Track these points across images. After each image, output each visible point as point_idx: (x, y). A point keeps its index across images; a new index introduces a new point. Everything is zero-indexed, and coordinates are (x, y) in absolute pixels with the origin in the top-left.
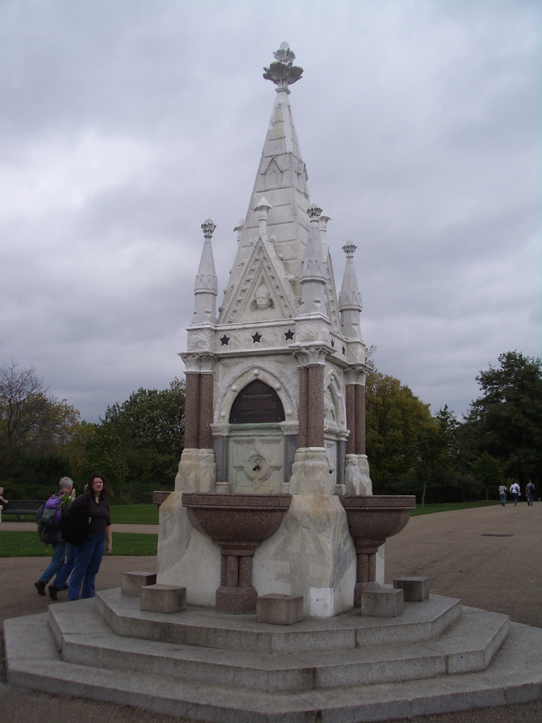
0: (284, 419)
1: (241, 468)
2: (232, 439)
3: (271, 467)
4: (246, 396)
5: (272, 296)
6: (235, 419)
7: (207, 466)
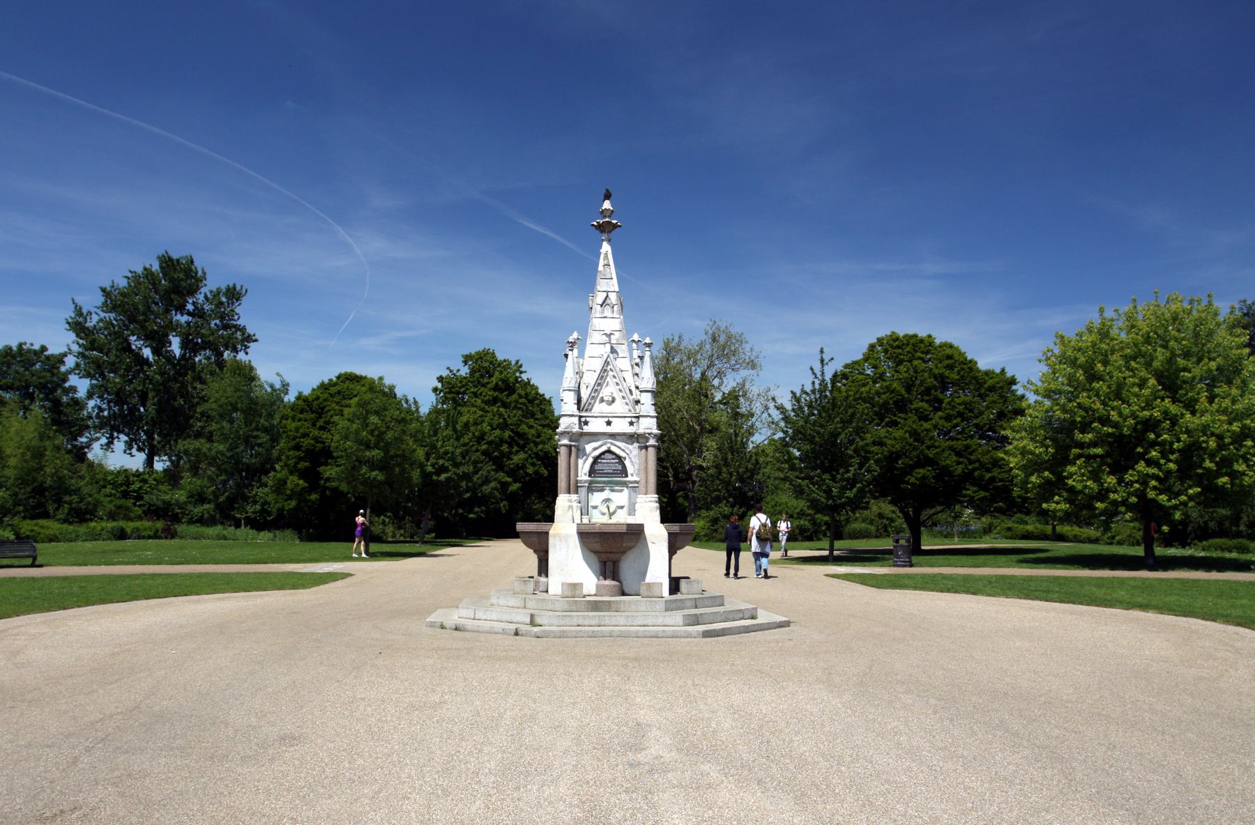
1: (595, 507)
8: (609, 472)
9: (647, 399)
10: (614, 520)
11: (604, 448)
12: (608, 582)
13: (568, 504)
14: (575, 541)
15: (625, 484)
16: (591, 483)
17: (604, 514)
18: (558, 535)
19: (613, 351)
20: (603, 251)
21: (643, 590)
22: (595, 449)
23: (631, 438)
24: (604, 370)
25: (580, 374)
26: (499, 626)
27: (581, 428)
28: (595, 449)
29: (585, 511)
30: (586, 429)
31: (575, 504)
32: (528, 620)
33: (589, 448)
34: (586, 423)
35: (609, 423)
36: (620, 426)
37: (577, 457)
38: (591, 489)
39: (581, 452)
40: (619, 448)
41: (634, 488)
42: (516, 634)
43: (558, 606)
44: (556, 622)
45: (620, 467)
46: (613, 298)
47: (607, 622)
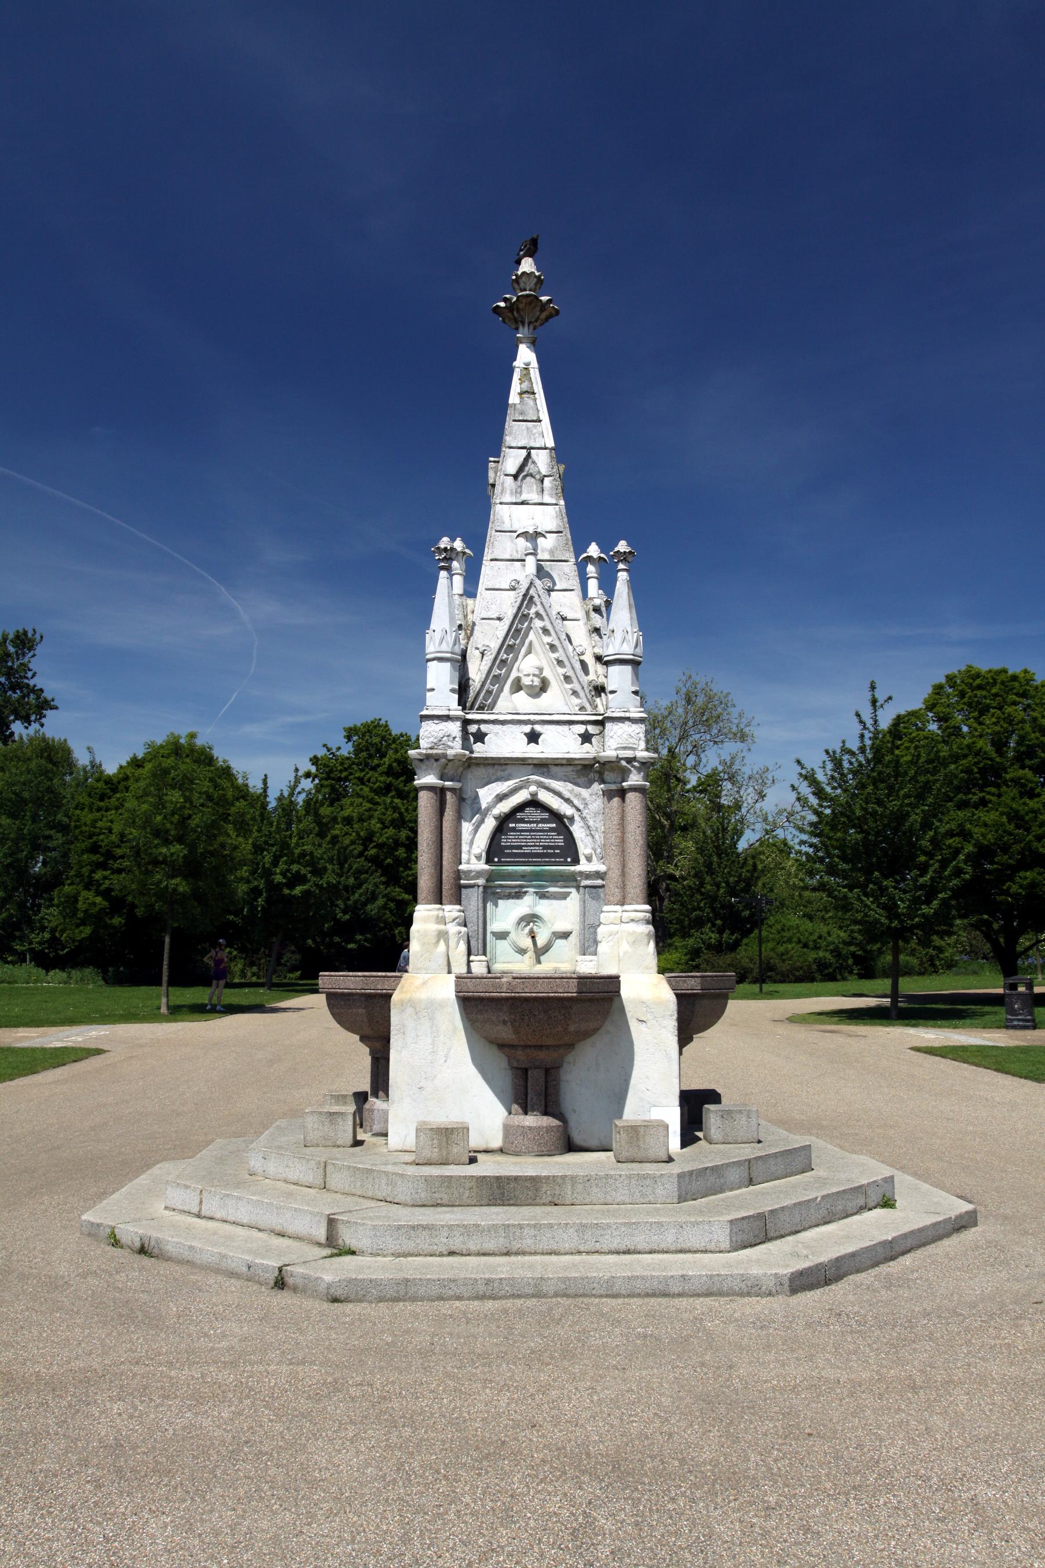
0: (576, 861)
1: (502, 936)
2: (489, 891)
5: (547, 673)
6: (496, 860)
8: (534, 851)
9: (620, 678)
10: (548, 966)
11: (522, 796)
12: (532, 1120)
13: (434, 927)
14: (452, 1019)
15: (572, 880)
16: (491, 877)
17: (522, 951)
18: (412, 1003)
19: (541, 572)
20: (518, 363)
21: (619, 1141)
22: (501, 798)
24: (521, 616)
25: (466, 629)
26: (238, 1257)
27: (466, 745)
28: (501, 798)
29: (477, 943)
30: (480, 750)
31: (453, 929)
32: (321, 1234)
33: (486, 795)
34: (480, 737)
35: (533, 737)
36: (561, 744)
37: (459, 818)
38: (492, 893)
41: (594, 888)
42: (280, 1283)
43: (403, 1192)
44: (391, 1244)
45: (560, 841)
46: (542, 461)
47: (528, 1243)
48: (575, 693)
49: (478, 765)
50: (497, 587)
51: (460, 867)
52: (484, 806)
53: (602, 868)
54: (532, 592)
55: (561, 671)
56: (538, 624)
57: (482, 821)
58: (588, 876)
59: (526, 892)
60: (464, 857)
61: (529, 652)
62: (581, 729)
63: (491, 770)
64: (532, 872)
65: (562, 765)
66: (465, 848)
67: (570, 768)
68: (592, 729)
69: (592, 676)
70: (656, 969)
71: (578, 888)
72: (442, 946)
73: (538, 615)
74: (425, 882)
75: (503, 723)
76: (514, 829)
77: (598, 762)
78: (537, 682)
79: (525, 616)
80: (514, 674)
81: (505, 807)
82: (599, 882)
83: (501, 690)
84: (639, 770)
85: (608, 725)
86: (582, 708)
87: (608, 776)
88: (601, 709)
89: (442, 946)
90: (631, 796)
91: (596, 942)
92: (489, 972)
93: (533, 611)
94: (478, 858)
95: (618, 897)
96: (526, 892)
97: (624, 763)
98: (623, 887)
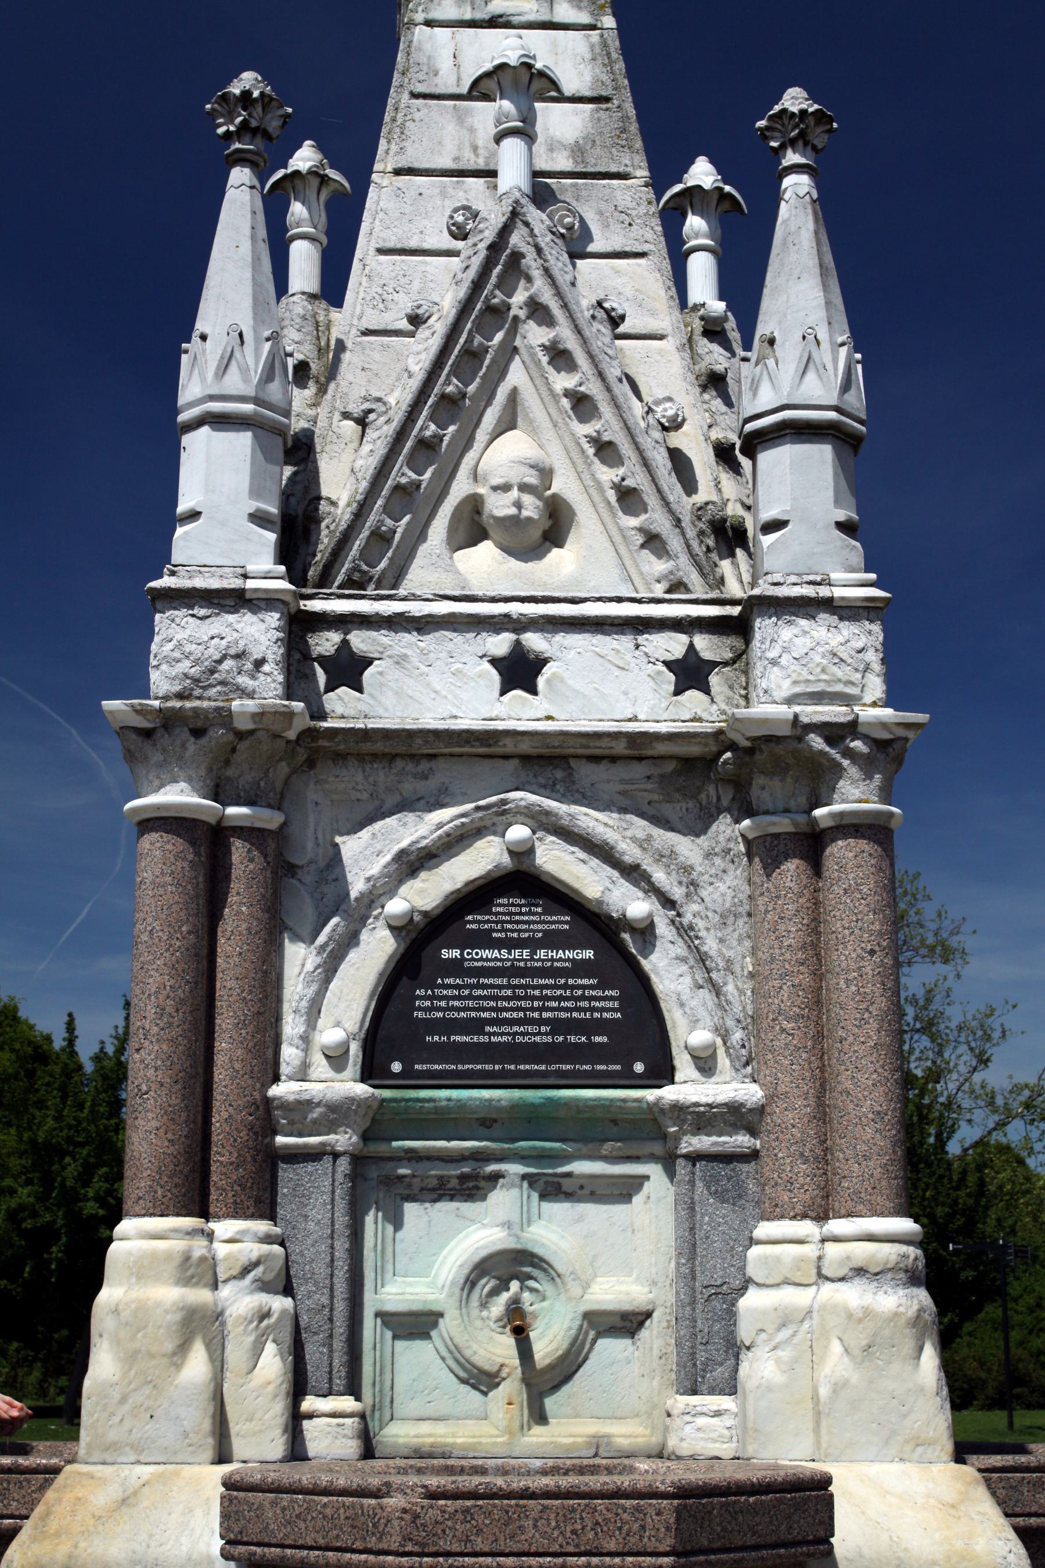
0: (663, 1072)
2: (373, 1172)
3: (592, 1318)
4: (455, 953)
5: (564, 485)
6: (396, 1067)
7: (265, 1315)
8: (522, 1042)
9: (799, 485)
10: (571, 1427)
11: (484, 857)
13: (169, 1294)
15: (650, 1135)
16: (377, 1124)
17: (483, 1380)
22: (413, 863)
23: (684, 778)
28: (413, 863)
29: (329, 1350)
30: (344, 708)
31: (240, 1301)
33: (365, 854)
34: (349, 670)
35: (520, 672)
36: (608, 690)
37: (273, 930)
38: (385, 1175)
39: (302, 890)
40: (597, 856)
41: (727, 1169)
48: (652, 541)
49: (340, 757)
50: (413, 243)
51: (275, 1091)
52: (357, 887)
53: (751, 1093)
54: (517, 239)
55: (608, 475)
56: (535, 335)
57: (350, 940)
58: (703, 1118)
59: (497, 1176)
60: (290, 1054)
61: (508, 423)
62: (674, 645)
63: (381, 775)
64: (516, 1107)
65: (614, 759)
66: (292, 1026)
67: (640, 770)
68: (705, 645)
69: (704, 494)
70: (948, 1446)
71: (669, 1162)
72: (197, 1365)
73: (537, 310)
74: (148, 1136)
75: (424, 625)
76: (456, 968)
77: (732, 746)
78: (532, 507)
79: (497, 313)
80: (460, 488)
81: (426, 892)
82: (742, 1141)
83: (419, 534)
84: (867, 765)
85: (763, 626)
86: (677, 586)
87: (766, 789)
88: (734, 589)
89: (197, 1365)
90: (841, 852)
91: (734, 1349)
92: (368, 1452)
93: (519, 298)
94: (336, 1059)
95: (806, 1194)
96: (497, 1176)
97: (817, 742)
98: (823, 1157)
